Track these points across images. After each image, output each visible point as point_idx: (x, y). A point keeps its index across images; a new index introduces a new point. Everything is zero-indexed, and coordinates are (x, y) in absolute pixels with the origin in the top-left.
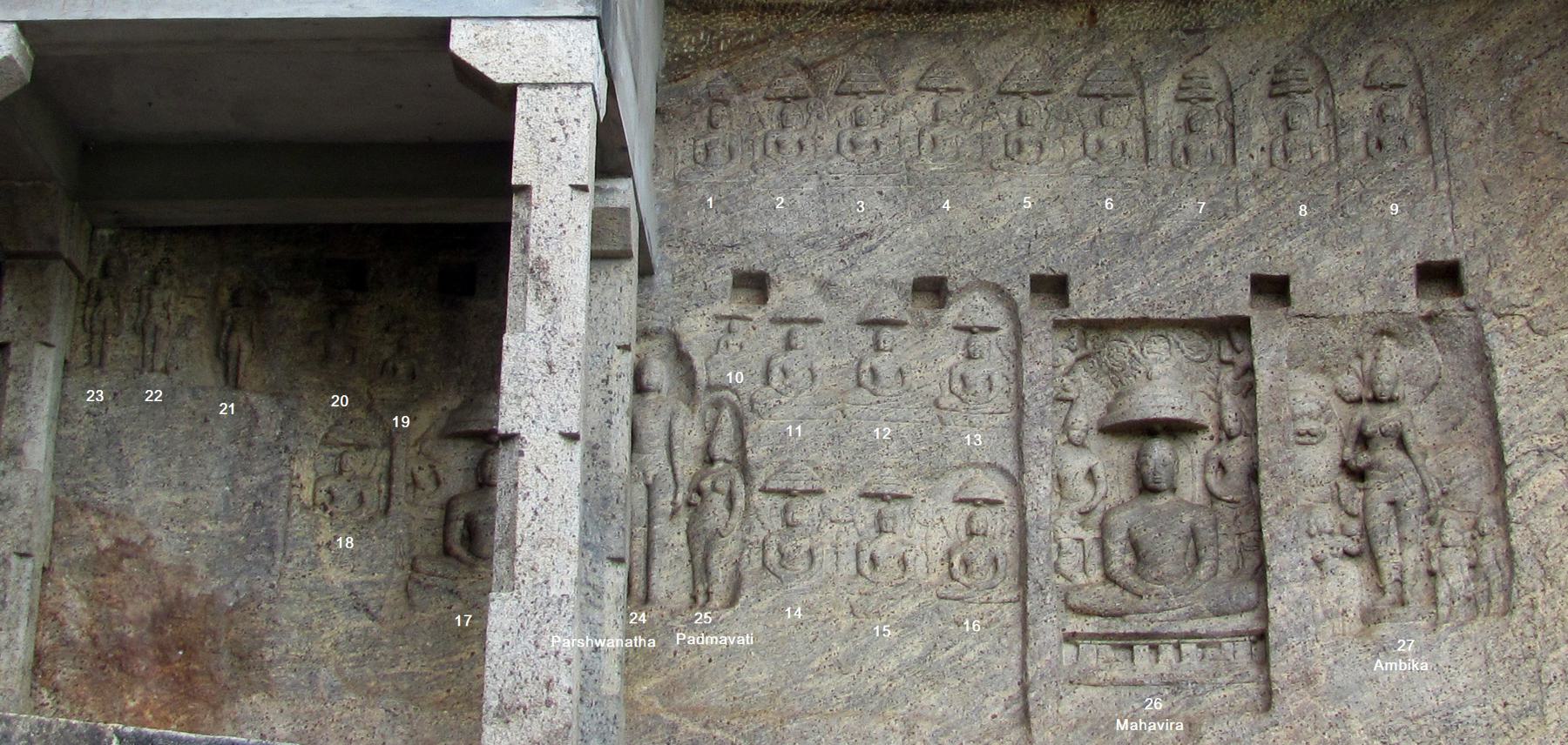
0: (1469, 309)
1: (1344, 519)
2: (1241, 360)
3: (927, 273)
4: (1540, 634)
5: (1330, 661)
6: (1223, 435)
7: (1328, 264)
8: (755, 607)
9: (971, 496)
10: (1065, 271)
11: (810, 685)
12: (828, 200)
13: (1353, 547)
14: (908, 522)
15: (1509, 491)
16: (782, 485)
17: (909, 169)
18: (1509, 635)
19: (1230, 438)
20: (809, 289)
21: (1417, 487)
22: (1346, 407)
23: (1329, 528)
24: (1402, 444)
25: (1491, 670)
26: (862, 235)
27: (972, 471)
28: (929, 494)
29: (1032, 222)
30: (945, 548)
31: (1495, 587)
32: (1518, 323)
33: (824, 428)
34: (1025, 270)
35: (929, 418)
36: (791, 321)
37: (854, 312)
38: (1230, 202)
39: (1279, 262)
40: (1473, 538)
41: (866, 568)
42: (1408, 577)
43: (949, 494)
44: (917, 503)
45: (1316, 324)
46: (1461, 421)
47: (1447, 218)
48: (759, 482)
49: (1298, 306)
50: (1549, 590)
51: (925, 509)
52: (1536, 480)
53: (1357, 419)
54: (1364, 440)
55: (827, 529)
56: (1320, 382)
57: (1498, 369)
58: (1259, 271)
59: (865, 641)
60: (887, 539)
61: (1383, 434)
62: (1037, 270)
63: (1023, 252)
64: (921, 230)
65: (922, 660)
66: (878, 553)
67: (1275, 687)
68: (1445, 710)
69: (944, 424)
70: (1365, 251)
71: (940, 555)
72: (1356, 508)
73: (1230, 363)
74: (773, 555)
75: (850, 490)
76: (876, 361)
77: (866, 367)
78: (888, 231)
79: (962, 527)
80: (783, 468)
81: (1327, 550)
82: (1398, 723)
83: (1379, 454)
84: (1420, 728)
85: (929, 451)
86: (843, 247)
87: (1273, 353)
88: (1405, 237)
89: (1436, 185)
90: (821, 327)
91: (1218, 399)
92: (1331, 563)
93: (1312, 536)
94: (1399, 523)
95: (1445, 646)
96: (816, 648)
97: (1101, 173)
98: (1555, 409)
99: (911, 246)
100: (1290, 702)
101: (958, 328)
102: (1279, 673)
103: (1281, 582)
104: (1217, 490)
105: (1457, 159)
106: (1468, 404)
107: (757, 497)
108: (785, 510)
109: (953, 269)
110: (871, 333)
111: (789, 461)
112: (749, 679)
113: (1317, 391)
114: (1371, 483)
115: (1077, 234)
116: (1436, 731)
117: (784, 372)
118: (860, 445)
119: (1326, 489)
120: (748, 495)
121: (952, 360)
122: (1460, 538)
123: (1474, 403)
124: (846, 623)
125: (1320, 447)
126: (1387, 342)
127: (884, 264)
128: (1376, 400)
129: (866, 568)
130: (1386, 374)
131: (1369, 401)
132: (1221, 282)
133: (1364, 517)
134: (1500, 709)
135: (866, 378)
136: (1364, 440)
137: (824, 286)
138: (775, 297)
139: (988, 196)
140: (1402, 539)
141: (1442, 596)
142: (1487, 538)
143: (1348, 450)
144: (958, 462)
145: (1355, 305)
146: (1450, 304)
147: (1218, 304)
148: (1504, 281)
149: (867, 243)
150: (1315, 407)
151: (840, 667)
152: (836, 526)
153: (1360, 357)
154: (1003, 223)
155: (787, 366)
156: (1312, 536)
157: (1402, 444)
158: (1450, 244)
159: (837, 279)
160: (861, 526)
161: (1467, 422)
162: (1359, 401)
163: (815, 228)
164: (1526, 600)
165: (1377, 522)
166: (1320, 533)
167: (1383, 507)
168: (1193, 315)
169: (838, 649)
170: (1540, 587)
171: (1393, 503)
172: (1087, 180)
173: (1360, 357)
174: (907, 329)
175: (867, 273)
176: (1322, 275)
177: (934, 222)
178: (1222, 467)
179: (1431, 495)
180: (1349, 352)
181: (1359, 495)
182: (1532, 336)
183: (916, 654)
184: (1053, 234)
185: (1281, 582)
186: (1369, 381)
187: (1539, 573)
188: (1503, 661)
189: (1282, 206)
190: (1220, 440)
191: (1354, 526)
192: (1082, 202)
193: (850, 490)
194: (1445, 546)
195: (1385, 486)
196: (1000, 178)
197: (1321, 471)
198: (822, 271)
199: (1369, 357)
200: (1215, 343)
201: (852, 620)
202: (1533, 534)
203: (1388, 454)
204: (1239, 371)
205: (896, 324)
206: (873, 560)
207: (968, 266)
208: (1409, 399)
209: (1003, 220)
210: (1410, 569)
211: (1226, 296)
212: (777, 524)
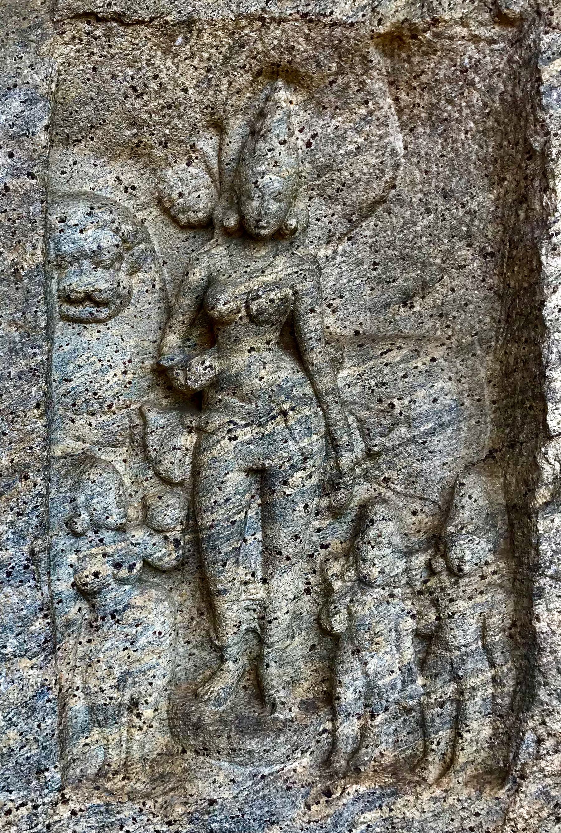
1: (152, 488)
13: (165, 555)
21: (314, 443)
22: (176, 238)
23: (114, 519)
24: (292, 341)
42: (276, 633)
45: (123, 40)
46: (425, 288)
53: (198, 275)
54: (208, 328)
56: (128, 178)
61: (252, 318)
72: (177, 466)
81: (107, 570)
83: (240, 360)
87: (16, 106)
92: (113, 595)
93: (77, 535)
94: (268, 515)
106: (448, 254)
113: (120, 197)
114: (217, 420)
119: (120, 420)
122: (401, 564)
123: (465, 253)
125: (115, 328)
128: (245, 235)
131: (227, 233)
133: (195, 488)
140: (271, 553)
141: (348, 696)
143: (173, 339)
150: (107, 239)
153: (219, 126)
156: (77, 535)
157: (292, 341)
161: (439, 293)
162: (206, 227)
165: (220, 515)
166: (97, 527)
167: (236, 479)
173: (219, 126)
179: (346, 460)
180: (195, 115)
181: (187, 440)
191: (171, 511)
194: (365, 583)
195: (245, 434)
197: (113, 380)
199: (237, 126)
203: (261, 365)
208: (315, 232)
210: (282, 616)
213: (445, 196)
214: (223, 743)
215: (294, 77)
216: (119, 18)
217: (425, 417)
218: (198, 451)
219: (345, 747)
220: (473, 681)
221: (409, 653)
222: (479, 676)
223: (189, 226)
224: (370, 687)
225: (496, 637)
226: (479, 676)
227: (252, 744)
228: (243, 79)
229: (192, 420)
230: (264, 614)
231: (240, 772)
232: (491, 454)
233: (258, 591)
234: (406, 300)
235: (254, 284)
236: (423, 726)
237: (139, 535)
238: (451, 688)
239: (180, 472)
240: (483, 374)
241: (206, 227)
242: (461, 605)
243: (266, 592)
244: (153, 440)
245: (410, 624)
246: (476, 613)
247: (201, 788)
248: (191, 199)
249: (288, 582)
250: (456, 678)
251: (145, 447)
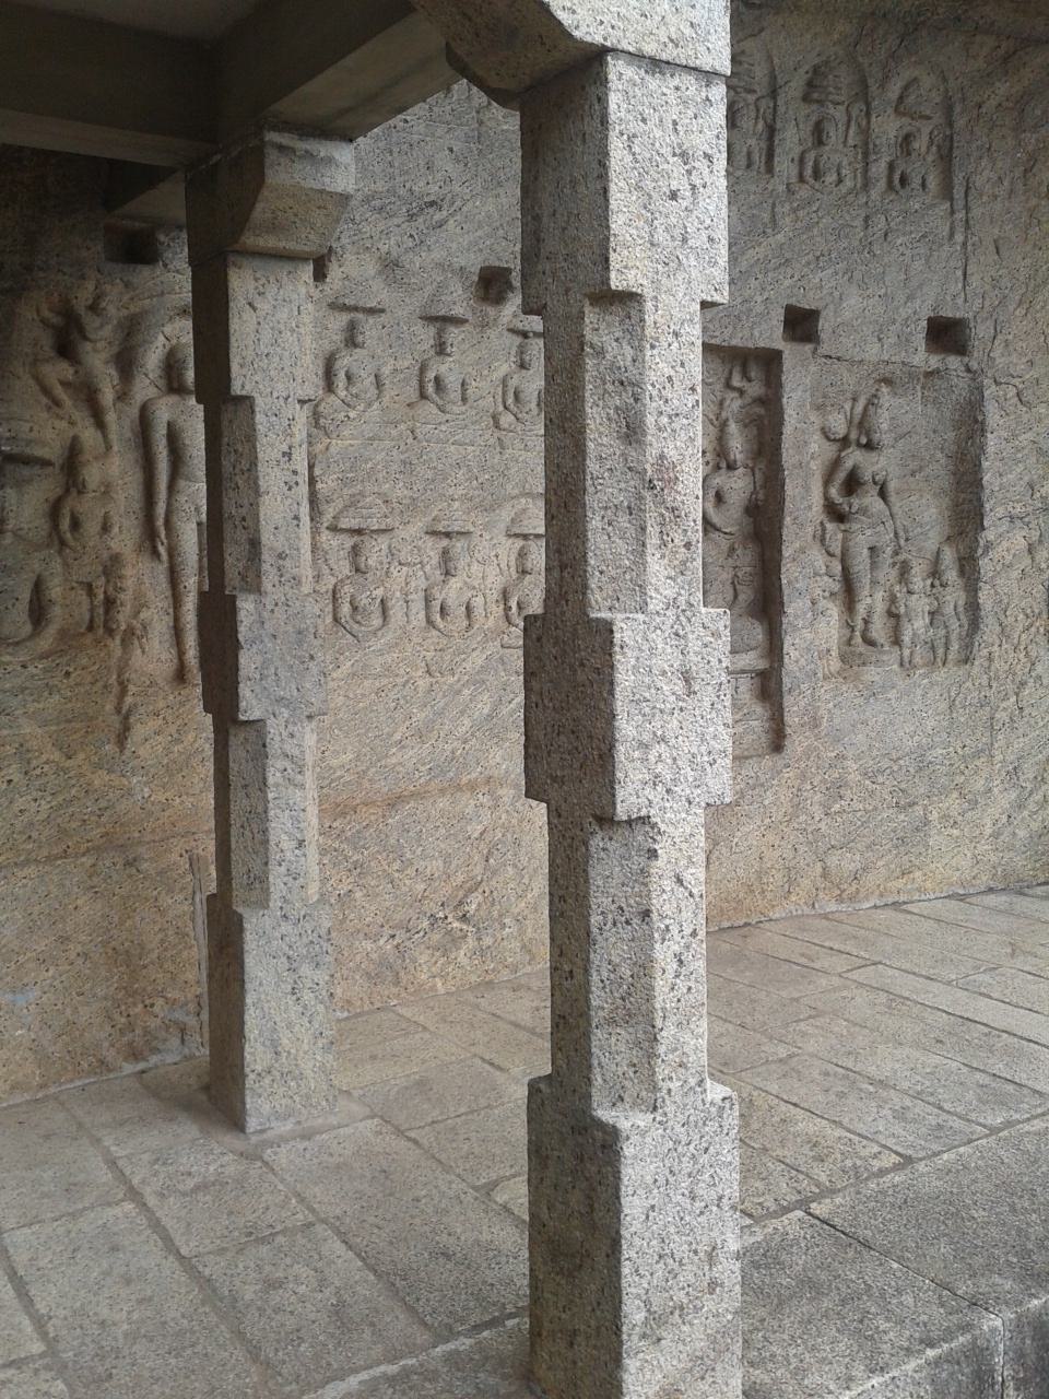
0: (968, 370)
2: (755, 389)
4: (994, 685)
5: (831, 705)
6: (724, 465)
7: (853, 302)
8: (334, 675)
9: (526, 532)
11: (394, 760)
14: (468, 559)
15: (980, 551)
16: (354, 523)
17: (481, 123)
18: (969, 684)
19: (731, 467)
20: (371, 268)
24: (883, 494)
25: (954, 715)
26: (432, 204)
27: (523, 501)
28: (487, 527)
30: (498, 586)
31: (954, 637)
32: (1012, 392)
33: (395, 452)
35: (491, 442)
36: (356, 309)
37: (415, 303)
38: (766, 216)
39: (811, 293)
40: (933, 586)
41: (437, 618)
43: (502, 526)
44: (475, 539)
45: (837, 365)
46: (921, 469)
47: (959, 273)
48: (327, 519)
49: (824, 349)
50: (1005, 646)
51: (483, 547)
52: (1005, 544)
53: (849, 464)
55: (395, 573)
57: (989, 435)
58: (793, 301)
59: (442, 704)
60: (455, 583)
65: (490, 717)
66: (450, 602)
67: (788, 731)
68: (920, 752)
69: (503, 448)
70: (886, 294)
71: (495, 597)
72: (836, 548)
73: (741, 392)
74: (346, 609)
75: (417, 527)
76: (443, 369)
77: (431, 375)
79: (513, 563)
80: (353, 503)
82: (885, 763)
84: (900, 769)
85: (491, 480)
86: (411, 217)
88: (920, 286)
89: (952, 235)
90: (383, 318)
91: (723, 426)
92: (823, 603)
95: (919, 692)
96: (398, 715)
98: (1026, 479)
99: (480, 227)
100: (797, 743)
101: (511, 331)
102: (792, 718)
103: (796, 628)
104: (716, 520)
105: (976, 212)
107: (325, 536)
108: (355, 551)
110: (432, 331)
111: (361, 494)
112: (334, 762)
114: (855, 526)
116: (911, 770)
117: (349, 377)
118: (430, 474)
120: (315, 532)
121: (504, 369)
123: (939, 455)
124: (423, 683)
126: (885, 389)
127: (454, 246)
129: (437, 618)
130: (883, 422)
131: (859, 445)
132: (759, 308)
134: (959, 750)
135: (430, 389)
136: (852, 484)
137: (390, 265)
138: (335, 272)
141: (906, 639)
142: (949, 589)
143: (833, 492)
144: (516, 491)
145: (872, 352)
146: (954, 362)
147: (756, 333)
148: (1006, 351)
151: (420, 735)
152: (405, 569)
155: (354, 370)
157: (883, 494)
158: (960, 301)
159: (405, 259)
160: (427, 568)
161: (928, 470)
163: (380, 186)
164: (985, 652)
168: (734, 342)
169: (420, 716)
170: (998, 642)
171: (872, 549)
174: (467, 327)
175: (437, 255)
176: (847, 315)
178: (719, 498)
180: (849, 395)
182: (1019, 406)
183: (486, 711)
185: (796, 628)
186: (863, 424)
187: (998, 629)
188: (964, 707)
189: (815, 231)
190: (718, 468)
191: (837, 568)
193: (417, 527)
195: (868, 532)
200: (729, 366)
201: (429, 680)
202: (997, 593)
204: (748, 400)
205: (458, 321)
206: (443, 610)
211: (764, 326)
212: (345, 568)
213: (934, 432)
214: (873, 659)
215: (888, 381)
216: (838, 359)
217: (927, 524)
218: (845, 541)
219: (906, 660)
220: (953, 627)
221: (927, 621)
222: (954, 625)
223: (834, 440)
224: (914, 634)
225: (961, 609)
226: (954, 625)
227: (885, 658)
228: (871, 382)
229: (843, 527)
230: (870, 613)
231: (879, 670)
232: (948, 538)
233: (869, 600)
234: (913, 474)
235: (875, 468)
236: (933, 648)
237: (826, 578)
238: (944, 631)
239: (838, 552)
240: (944, 506)
241: (844, 442)
242: (948, 598)
243: (872, 601)
244: (828, 536)
245: (927, 608)
246: (954, 596)
247: (867, 678)
248: (838, 429)
249: (879, 595)
250: (946, 627)
251: (823, 540)
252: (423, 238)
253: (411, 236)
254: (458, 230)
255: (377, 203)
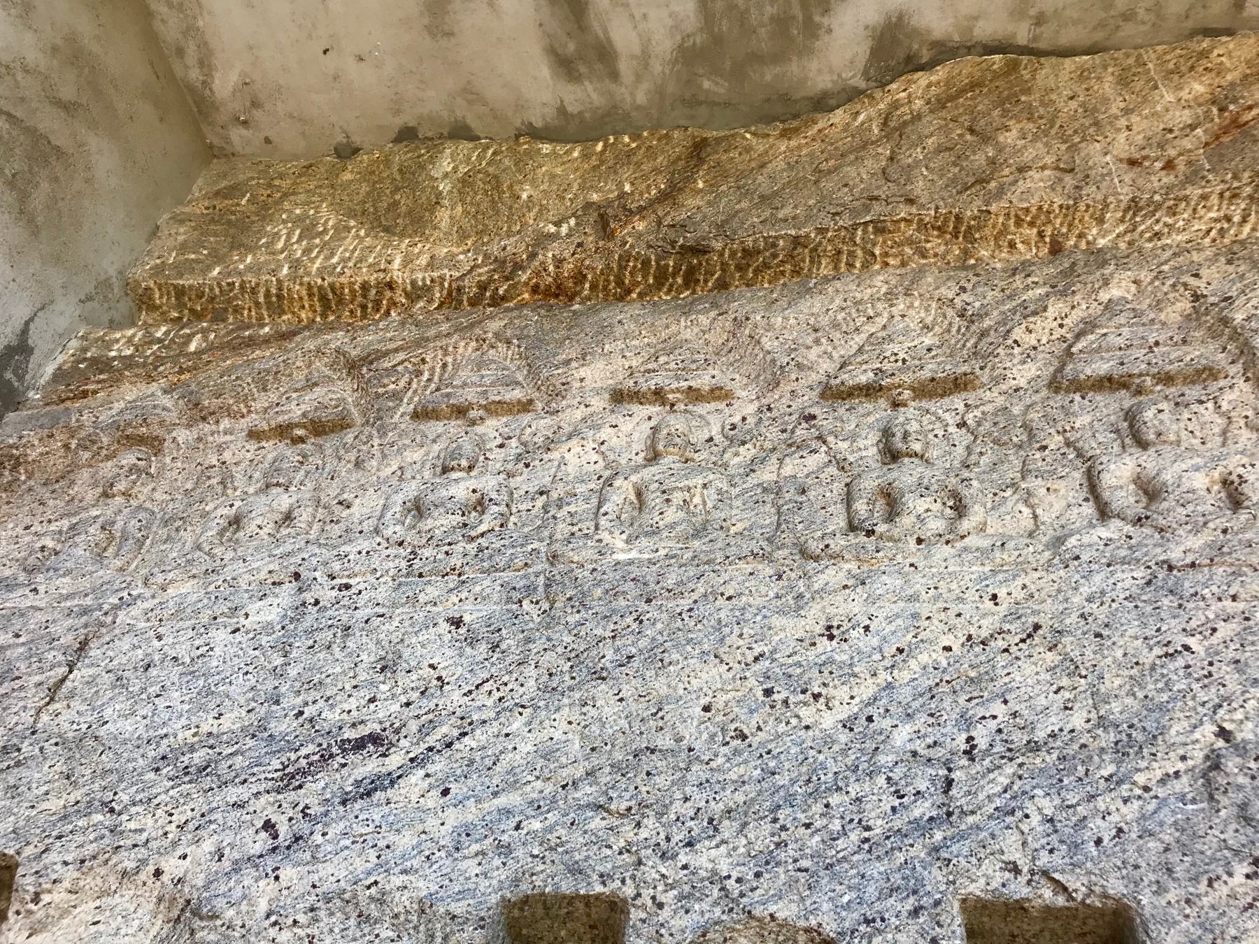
3: (552, 879)
10: (1116, 887)
12: (301, 643)
17: (554, 558)
26: (359, 745)
29: (950, 708)
34: (935, 877)
62: (985, 879)
63: (923, 809)
64: (560, 726)
78: (447, 729)
86: (290, 779)
97: (1175, 555)
109: (653, 869)
115: (1132, 744)
127: (405, 841)
139: (788, 629)
149: (367, 766)
154: (843, 713)
172: (1129, 578)
175: (333, 873)
177: (608, 708)
184: (1033, 747)
192: (1129, 638)
196: (832, 576)
198: (189, 864)
207: (705, 858)
209: (846, 700)
252: (304, 827)
253: (269, 826)
254: (433, 799)
255: (199, 757)
